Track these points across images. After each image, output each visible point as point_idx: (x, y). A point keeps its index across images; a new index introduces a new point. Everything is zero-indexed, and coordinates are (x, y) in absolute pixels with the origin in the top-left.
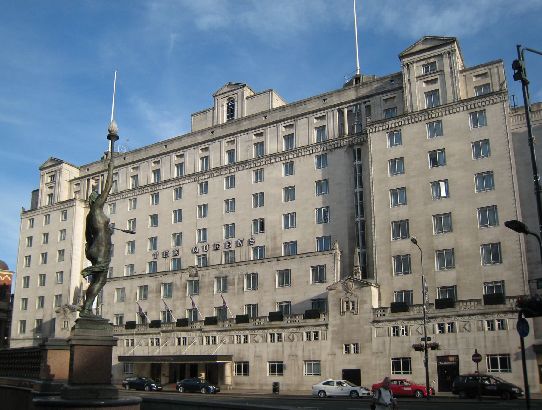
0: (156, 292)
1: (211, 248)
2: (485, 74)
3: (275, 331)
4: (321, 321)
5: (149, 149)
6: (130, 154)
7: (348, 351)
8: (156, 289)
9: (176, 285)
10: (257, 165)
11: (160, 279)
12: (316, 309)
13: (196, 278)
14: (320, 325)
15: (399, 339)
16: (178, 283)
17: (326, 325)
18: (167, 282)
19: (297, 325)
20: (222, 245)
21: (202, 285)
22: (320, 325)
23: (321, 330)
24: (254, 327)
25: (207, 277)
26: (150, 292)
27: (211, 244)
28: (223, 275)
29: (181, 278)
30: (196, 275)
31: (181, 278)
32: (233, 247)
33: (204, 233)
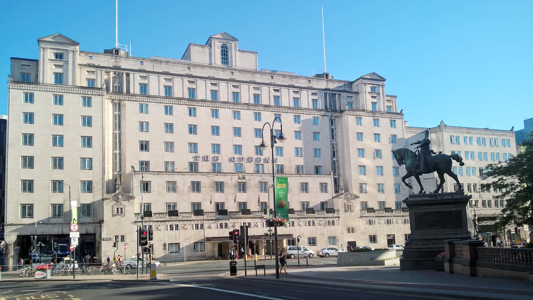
0: (210, 188)
1: (201, 159)
2: (297, 92)
3: (311, 220)
4: (336, 215)
5: (171, 64)
6: (149, 61)
7: (349, 232)
8: (209, 185)
9: (227, 184)
10: (58, 91)
11: (213, 178)
12: (326, 208)
13: (244, 181)
14: (335, 217)
15: (372, 226)
16: (230, 183)
17: (339, 217)
18: (219, 181)
19: (323, 216)
20: (210, 159)
21: (249, 186)
22: (335, 217)
23: (336, 220)
24: (298, 217)
25: (253, 180)
26: (204, 187)
27: (201, 156)
28: (265, 181)
29: (231, 179)
30: (244, 178)
31: (231, 179)
32: (262, 162)
33: (238, 148)
